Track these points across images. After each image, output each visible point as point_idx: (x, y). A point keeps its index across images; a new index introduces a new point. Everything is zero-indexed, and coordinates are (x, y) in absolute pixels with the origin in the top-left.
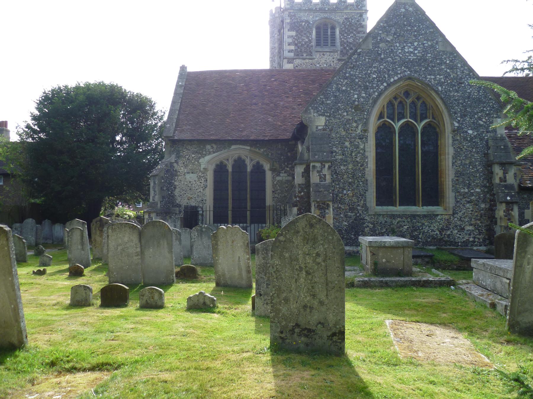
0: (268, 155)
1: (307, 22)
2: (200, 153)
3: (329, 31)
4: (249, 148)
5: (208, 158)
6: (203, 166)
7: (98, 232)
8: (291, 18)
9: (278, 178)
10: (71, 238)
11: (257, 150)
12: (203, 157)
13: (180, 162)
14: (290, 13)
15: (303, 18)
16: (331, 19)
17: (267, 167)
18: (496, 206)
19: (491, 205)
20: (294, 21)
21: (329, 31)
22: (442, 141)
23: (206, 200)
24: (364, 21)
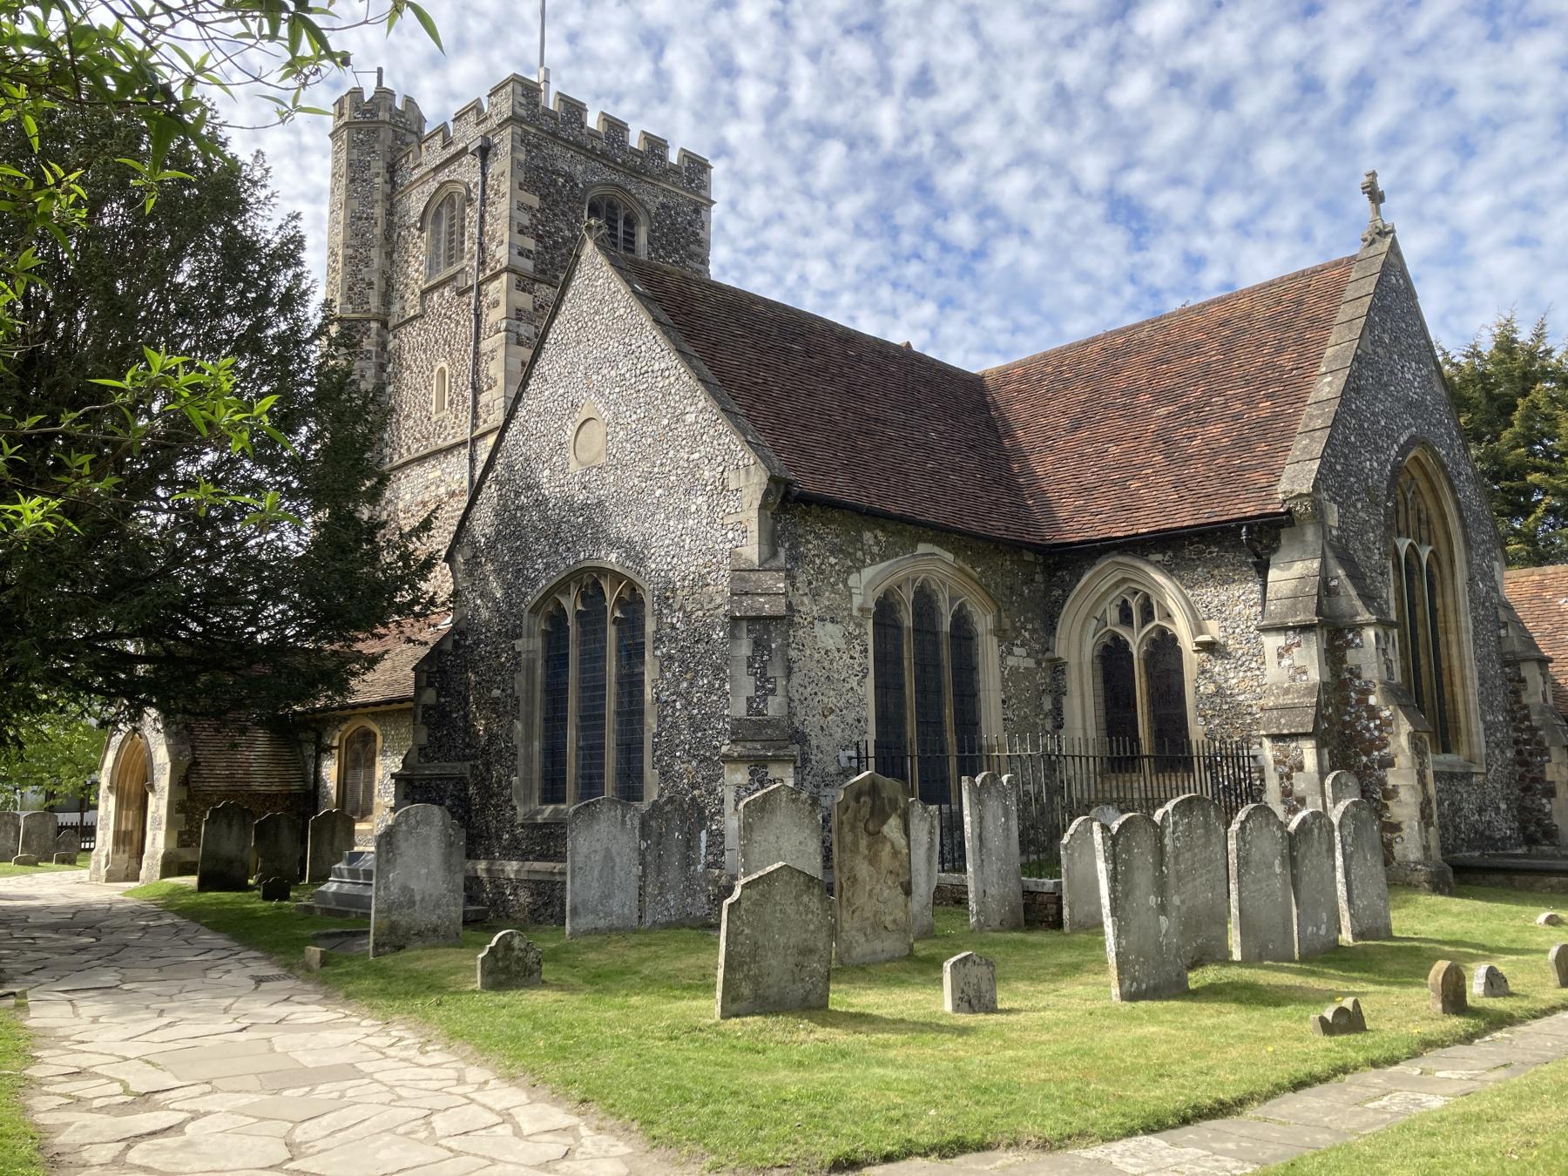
0: (988, 586)
1: (569, 178)
2: (848, 555)
3: (621, 224)
4: (949, 557)
5: (868, 573)
6: (857, 601)
8: (529, 152)
9: (1011, 661)
11: (968, 568)
12: (859, 570)
13: (802, 579)
14: (526, 133)
16: (629, 192)
17: (983, 622)
18: (1544, 751)
19: (1519, 752)
20: (535, 162)
21: (621, 224)
22: (1449, 600)
24: (702, 228)
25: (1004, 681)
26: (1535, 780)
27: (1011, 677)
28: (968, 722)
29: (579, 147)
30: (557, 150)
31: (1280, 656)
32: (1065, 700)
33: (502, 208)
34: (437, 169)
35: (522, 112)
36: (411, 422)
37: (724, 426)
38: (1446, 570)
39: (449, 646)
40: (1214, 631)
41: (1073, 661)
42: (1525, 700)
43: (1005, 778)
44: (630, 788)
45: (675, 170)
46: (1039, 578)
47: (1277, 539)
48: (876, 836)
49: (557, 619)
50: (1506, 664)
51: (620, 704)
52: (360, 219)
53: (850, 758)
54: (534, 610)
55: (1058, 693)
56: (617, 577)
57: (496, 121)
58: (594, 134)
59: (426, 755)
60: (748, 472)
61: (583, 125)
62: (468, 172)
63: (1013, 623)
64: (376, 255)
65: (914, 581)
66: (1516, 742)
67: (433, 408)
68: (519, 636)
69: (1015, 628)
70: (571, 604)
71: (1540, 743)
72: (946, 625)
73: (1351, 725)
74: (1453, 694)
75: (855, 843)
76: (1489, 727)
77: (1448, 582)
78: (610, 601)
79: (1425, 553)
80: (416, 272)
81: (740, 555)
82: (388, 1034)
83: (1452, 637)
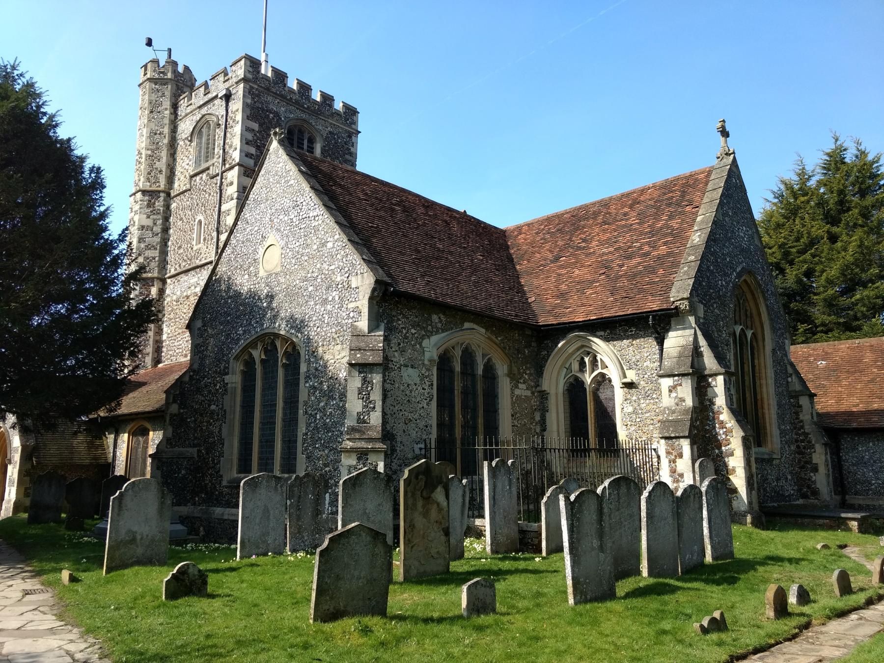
0: (505, 348)
1: (277, 114)
4: (483, 331)
5: (435, 339)
6: (427, 355)
7: (420, 504)
8: (253, 99)
10: (578, 519)
11: (494, 338)
12: (429, 337)
13: (394, 341)
14: (252, 88)
15: (271, 106)
16: (311, 124)
17: (501, 369)
18: (813, 447)
19: (798, 447)
22: (762, 360)
23: (431, 426)
24: (353, 146)
25: (513, 404)
26: (807, 462)
27: (517, 401)
28: (492, 429)
29: (283, 97)
30: (270, 99)
31: (670, 391)
32: (547, 415)
33: (237, 129)
34: (200, 107)
35: (250, 76)
36: (181, 251)
37: (350, 249)
38: (761, 343)
39: (187, 379)
40: (631, 376)
41: (552, 392)
42: (801, 417)
43: (510, 462)
44: (289, 465)
45: (337, 113)
46: (534, 344)
47: (669, 323)
48: (428, 499)
49: (250, 364)
50: (792, 397)
51: (285, 414)
52: (156, 134)
53: (421, 449)
54: (237, 358)
55: (544, 410)
56: (285, 339)
57: (235, 80)
58: (291, 91)
59: (171, 444)
60: (363, 277)
61: (285, 85)
62: (218, 108)
63: (519, 369)
64: (164, 154)
65: (462, 344)
66: (797, 441)
67: (194, 243)
68: (227, 374)
69: (519, 373)
70: (258, 354)
71: (810, 442)
72: (480, 370)
73: (710, 431)
74: (763, 414)
75: (415, 505)
76: (783, 433)
77: (762, 351)
78: (280, 355)
79: (749, 334)
80: (185, 164)
81: (357, 327)
82: (85, 641)
83: (764, 382)
